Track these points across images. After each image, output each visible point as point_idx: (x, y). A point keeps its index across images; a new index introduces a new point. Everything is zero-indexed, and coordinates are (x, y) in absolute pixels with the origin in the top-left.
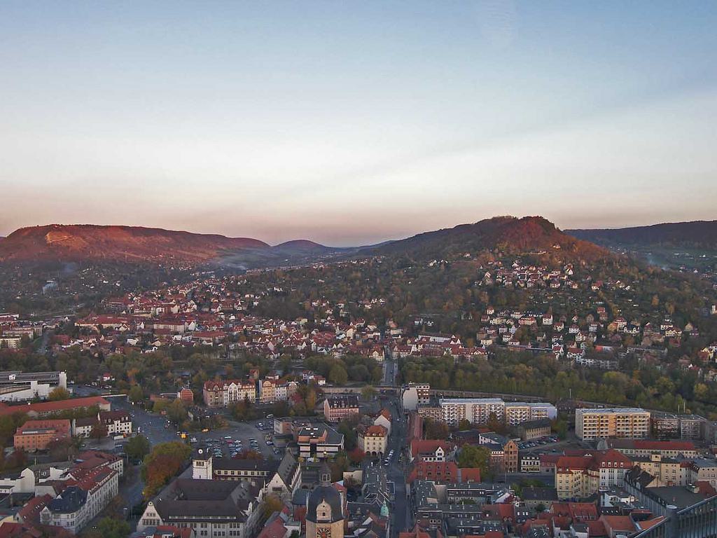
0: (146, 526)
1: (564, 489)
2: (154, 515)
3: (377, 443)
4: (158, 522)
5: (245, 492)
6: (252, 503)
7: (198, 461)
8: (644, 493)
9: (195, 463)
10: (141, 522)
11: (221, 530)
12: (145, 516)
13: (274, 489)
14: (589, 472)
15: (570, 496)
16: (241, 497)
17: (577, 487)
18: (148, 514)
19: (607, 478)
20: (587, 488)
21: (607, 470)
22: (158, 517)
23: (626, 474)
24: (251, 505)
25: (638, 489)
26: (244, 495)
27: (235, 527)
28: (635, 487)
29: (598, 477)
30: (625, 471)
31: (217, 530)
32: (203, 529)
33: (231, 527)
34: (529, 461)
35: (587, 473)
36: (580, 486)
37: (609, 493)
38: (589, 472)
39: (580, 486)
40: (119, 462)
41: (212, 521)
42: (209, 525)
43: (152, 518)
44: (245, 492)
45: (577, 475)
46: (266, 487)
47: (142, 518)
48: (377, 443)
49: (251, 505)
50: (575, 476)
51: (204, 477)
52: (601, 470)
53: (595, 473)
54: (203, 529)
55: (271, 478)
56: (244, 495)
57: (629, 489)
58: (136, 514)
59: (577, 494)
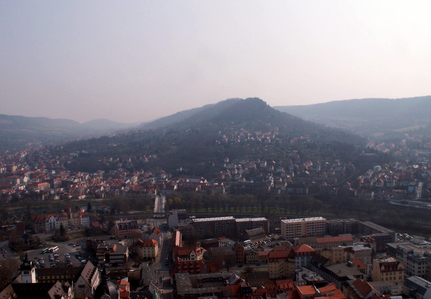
1: (273, 272)
3: (147, 251)
5: (58, 290)
13: (80, 286)
15: (277, 276)
16: (56, 294)
19: (300, 263)
20: (288, 270)
21: (300, 258)
23: (312, 259)
25: (319, 268)
26: (58, 291)
29: (295, 262)
30: (311, 257)
34: (249, 256)
36: (283, 269)
39: (283, 269)
44: (58, 290)
45: (282, 263)
48: (147, 251)
50: (280, 263)
51: (29, 282)
52: (296, 258)
56: (58, 291)
59: (282, 274)
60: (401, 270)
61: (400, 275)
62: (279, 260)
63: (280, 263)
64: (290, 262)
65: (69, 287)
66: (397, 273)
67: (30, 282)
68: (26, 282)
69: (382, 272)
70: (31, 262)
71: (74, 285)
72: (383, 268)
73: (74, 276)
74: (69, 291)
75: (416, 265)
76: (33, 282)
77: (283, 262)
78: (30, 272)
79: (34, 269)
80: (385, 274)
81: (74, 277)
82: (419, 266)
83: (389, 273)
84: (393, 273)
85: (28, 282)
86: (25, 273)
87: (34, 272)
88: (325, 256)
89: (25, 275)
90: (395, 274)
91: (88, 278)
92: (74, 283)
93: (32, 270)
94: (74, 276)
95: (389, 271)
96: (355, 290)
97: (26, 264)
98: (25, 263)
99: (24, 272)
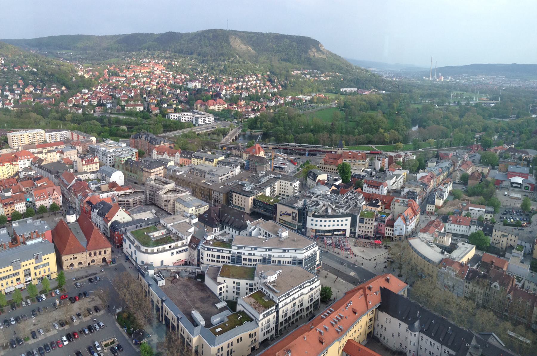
8: (40, 168)
14: (13, 163)
17: (8, 172)
21: (22, 161)
28: (36, 166)
35: (12, 164)
37: (23, 171)
38: (13, 163)
39: (10, 171)
45: (7, 166)
52: (19, 161)
53: (16, 163)
57: (34, 167)
60: (96, 163)
61: (97, 166)
62: (5, 164)
63: (6, 166)
64: (14, 165)
66: (94, 165)
69: (83, 165)
72: (84, 162)
75: (109, 159)
77: (9, 165)
80: (85, 166)
82: (110, 159)
83: (88, 165)
84: (91, 165)
88: (41, 158)
90: (92, 166)
95: (88, 164)
96: (63, 179)
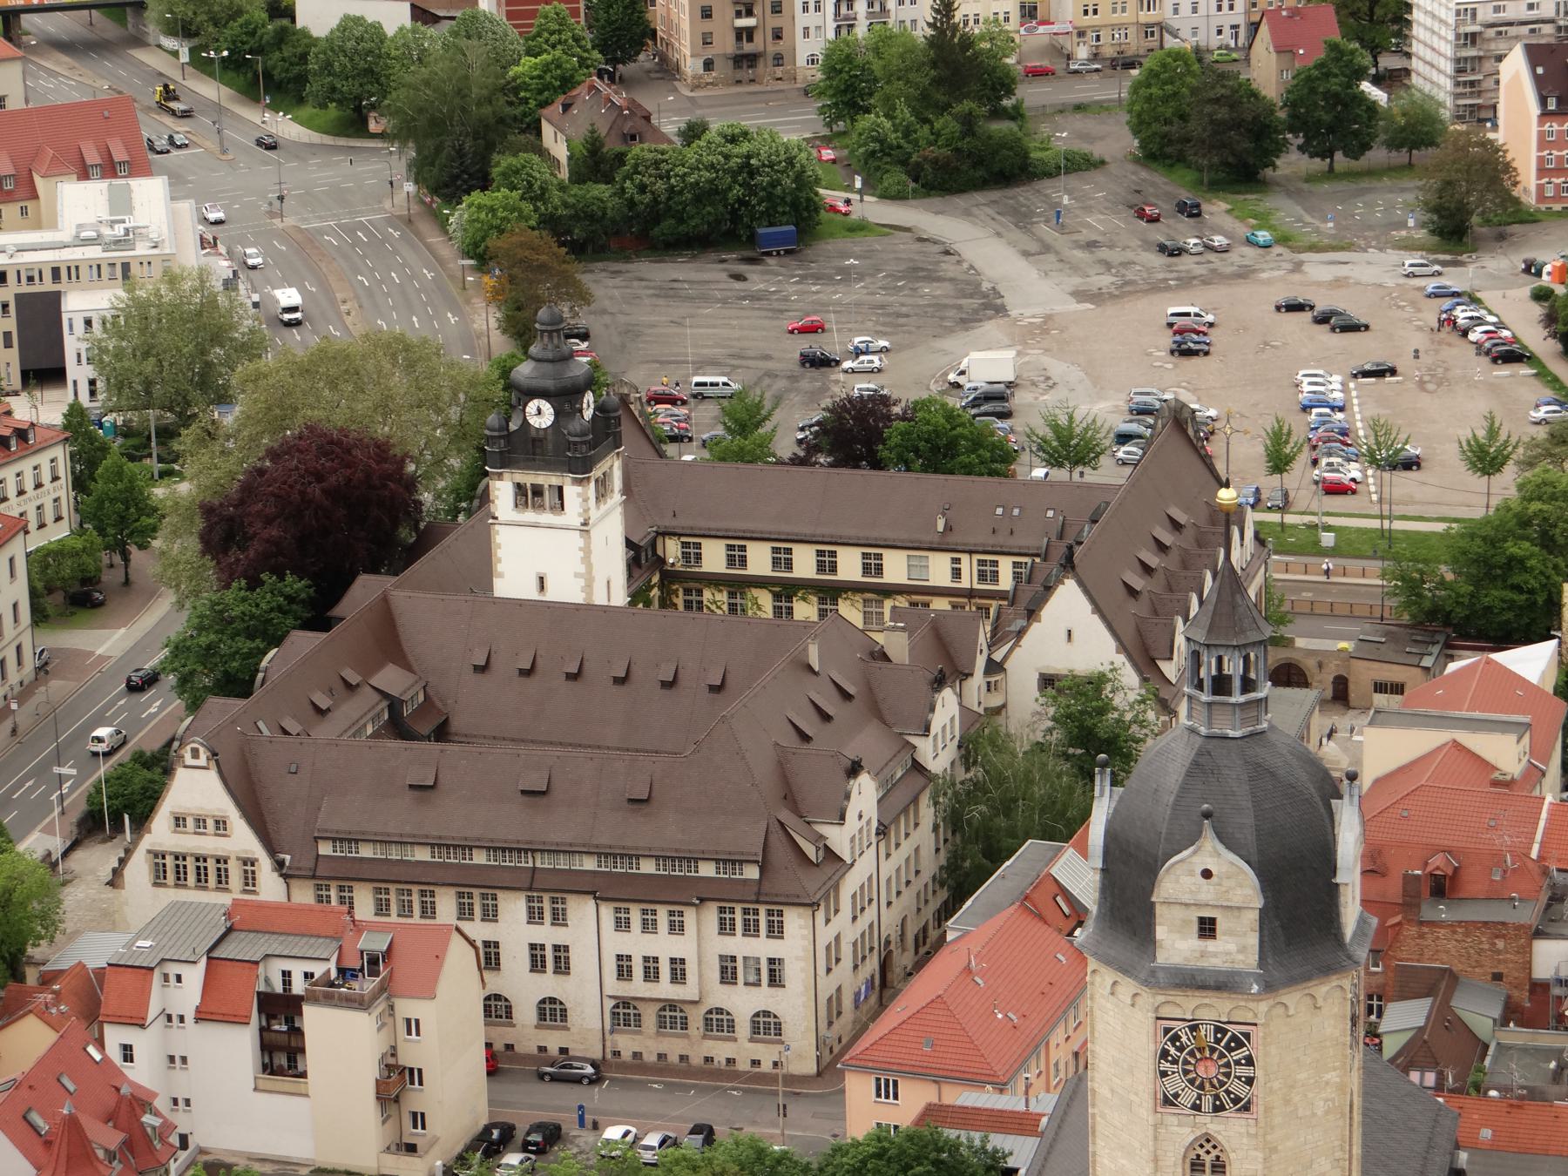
0: (171, 895)
2: (221, 825)
4: (250, 879)
6: (876, 775)
7: (529, 478)
9: (502, 491)
10: (139, 869)
11: (664, 945)
12: (160, 833)
18: (179, 821)
22: (242, 839)
24: (865, 795)
27: (751, 929)
31: (637, 944)
32: (547, 934)
33: (726, 928)
40: (43, 460)
41: (598, 889)
42: (582, 911)
43: (209, 844)
46: (994, 667)
47: (147, 842)
49: (865, 795)
51: (565, 590)
54: (547, 934)
55: (1032, 614)
58: (128, 807)
65: (939, 682)
67: (578, 598)
68: (530, 592)
70: (589, 397)
71: (994, 667)
73: (1006, 566)
74: (936, 727)
76: (600, 599)
78: (571, 492)
79: (613, 466)
81: (1006, 582)
85: (553, 594)
86: (528, 496)
87: (617, 497)
89: (530, 516)
91: (1139, 608)
92: (994, 643)
93: (597, 472)
94: (1006, 566)
97: (540, 415)
98: (532, 407)
99: (520, 489)
